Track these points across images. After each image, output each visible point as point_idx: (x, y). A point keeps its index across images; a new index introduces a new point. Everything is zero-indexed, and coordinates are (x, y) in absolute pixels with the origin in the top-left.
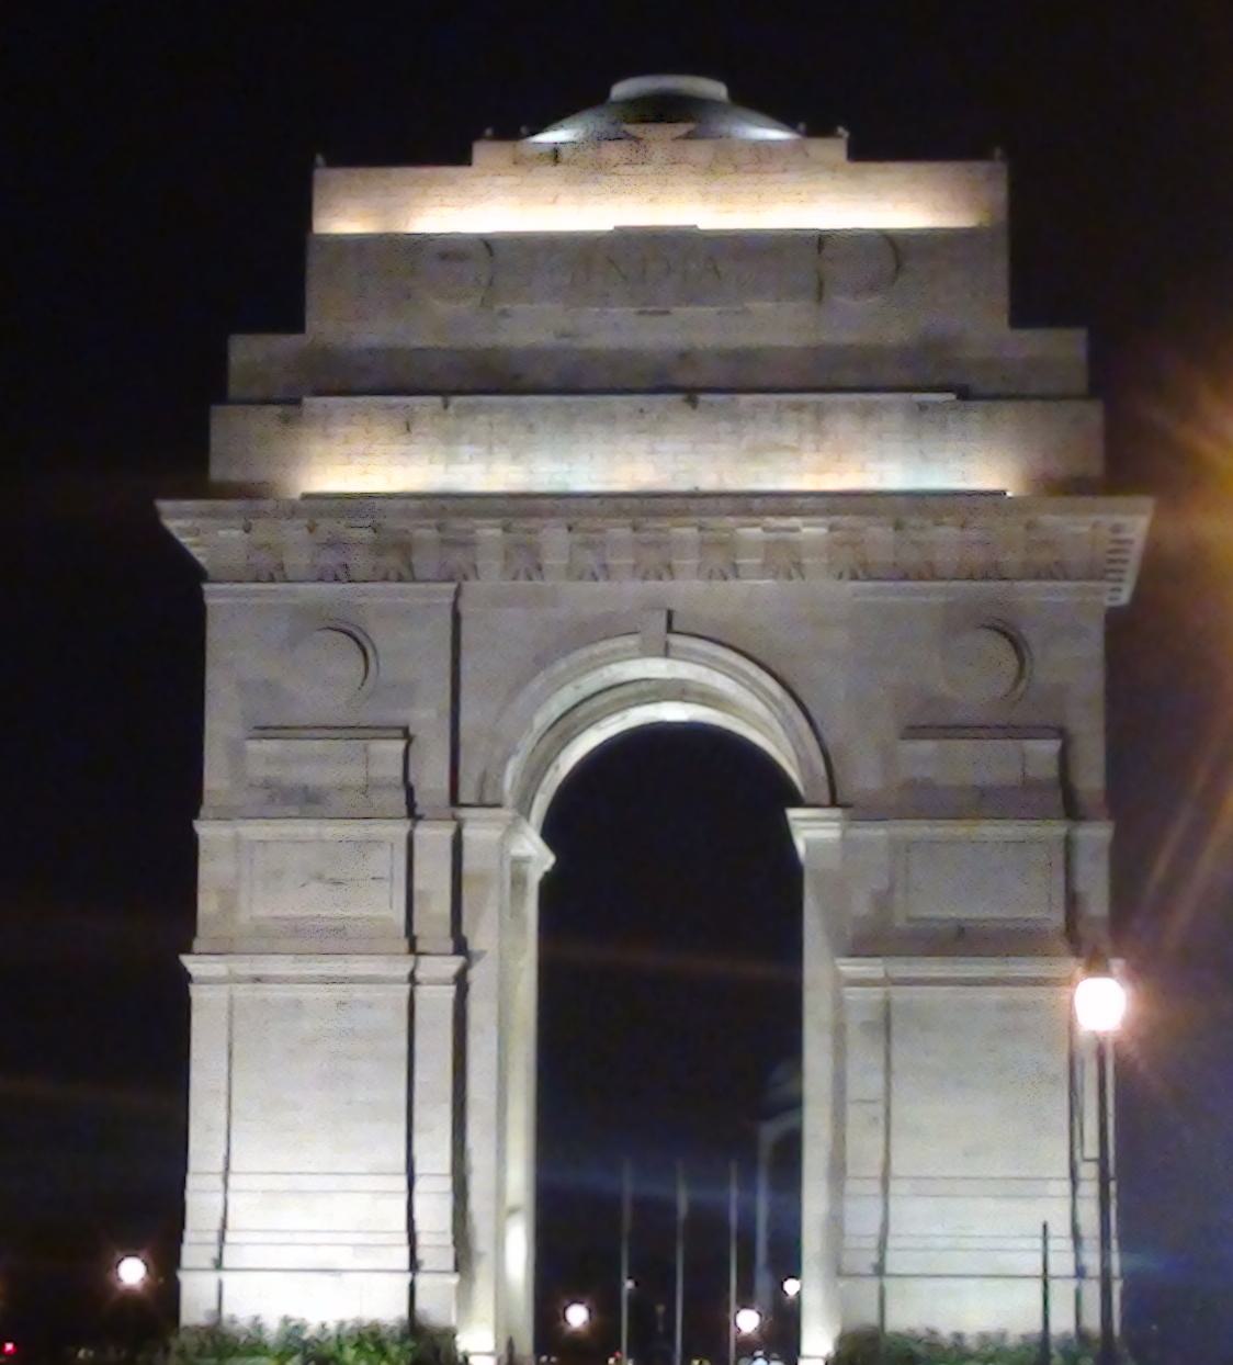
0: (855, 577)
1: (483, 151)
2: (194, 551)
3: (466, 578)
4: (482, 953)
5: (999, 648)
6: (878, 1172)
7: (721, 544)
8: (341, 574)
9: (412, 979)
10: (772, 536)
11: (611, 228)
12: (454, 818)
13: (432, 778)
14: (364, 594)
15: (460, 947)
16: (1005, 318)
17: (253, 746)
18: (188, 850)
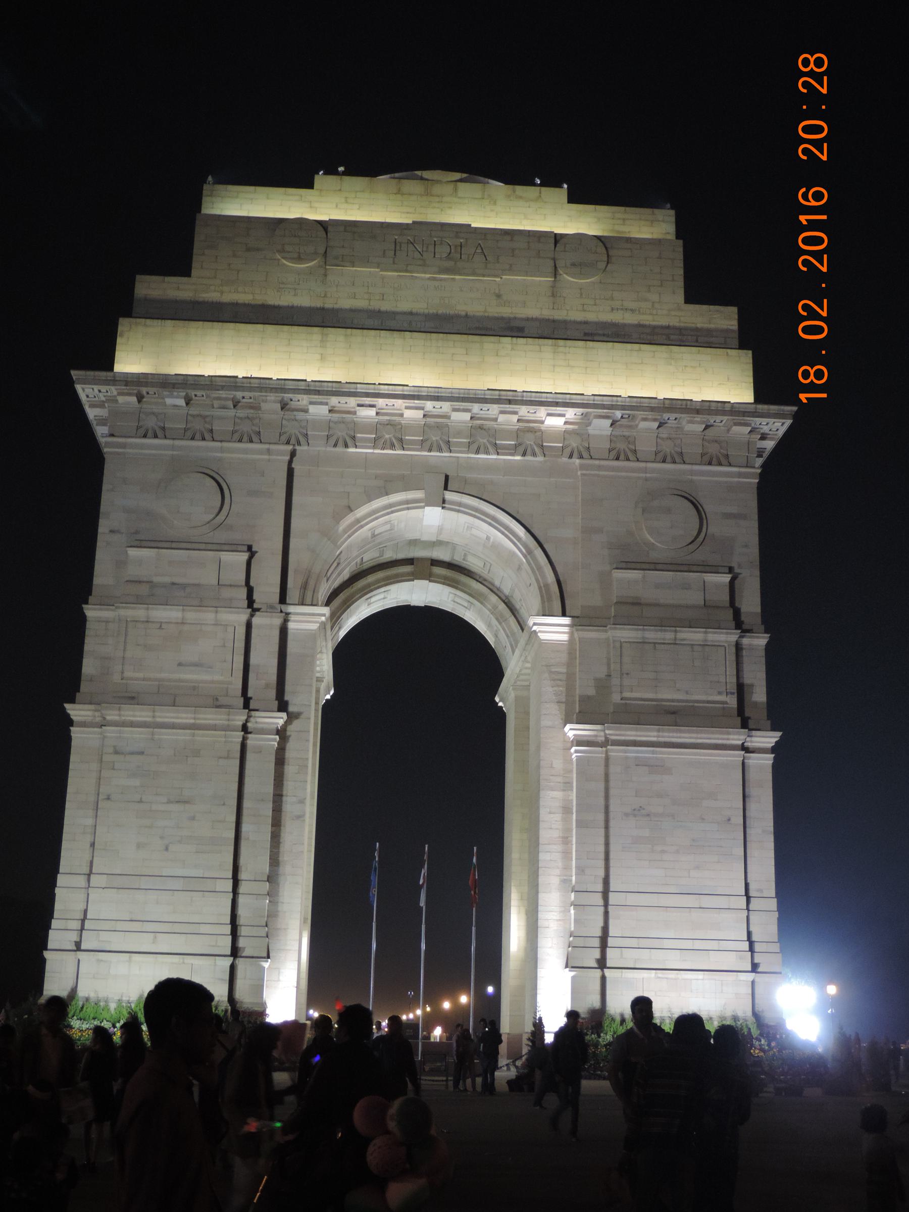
0: (581, 457)
1: (320, 179)
2: (100, 431)
3: (299, 444)
6: (600, 887)
8: (207, 436)
11: (408, 221)
12: (281, 612)
14: (222, 450)
15: (283, 706)
16: (680, 297)
17: (132, 552)
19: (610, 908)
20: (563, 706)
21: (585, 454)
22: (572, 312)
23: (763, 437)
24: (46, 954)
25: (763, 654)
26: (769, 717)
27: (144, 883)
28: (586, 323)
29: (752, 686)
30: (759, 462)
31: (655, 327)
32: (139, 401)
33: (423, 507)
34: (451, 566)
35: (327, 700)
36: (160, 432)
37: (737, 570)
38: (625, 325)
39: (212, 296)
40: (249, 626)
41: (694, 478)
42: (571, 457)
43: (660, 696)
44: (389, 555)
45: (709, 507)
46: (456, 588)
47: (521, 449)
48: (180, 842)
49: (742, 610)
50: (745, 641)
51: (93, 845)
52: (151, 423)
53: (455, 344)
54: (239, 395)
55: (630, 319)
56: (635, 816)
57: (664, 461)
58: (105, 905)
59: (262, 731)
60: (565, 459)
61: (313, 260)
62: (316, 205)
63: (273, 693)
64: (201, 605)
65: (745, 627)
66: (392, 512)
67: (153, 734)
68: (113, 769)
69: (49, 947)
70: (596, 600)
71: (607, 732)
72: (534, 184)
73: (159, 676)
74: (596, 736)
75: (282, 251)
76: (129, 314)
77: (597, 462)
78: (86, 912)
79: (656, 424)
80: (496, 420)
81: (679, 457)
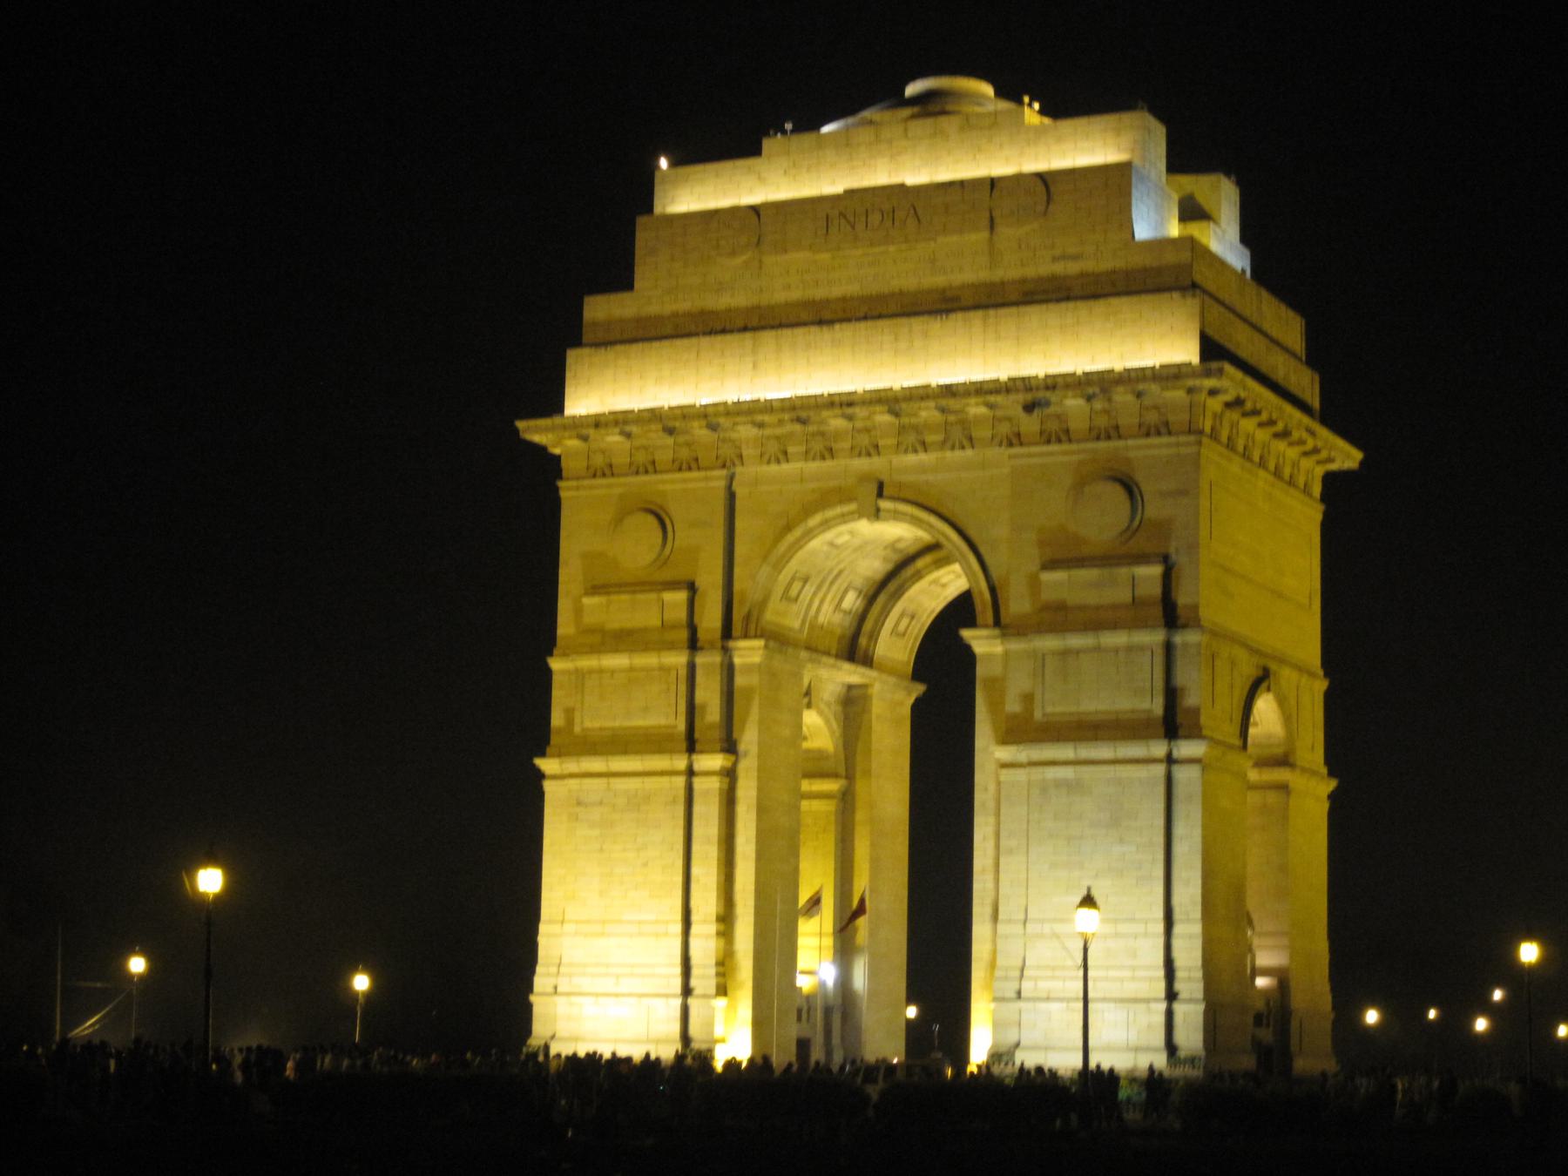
0: (1011, 444)
5: (1117, 493)
6: (1022, 917)
9: (690, 773)
13: (710, 619)
14: (664, 482)
17: (586, 601)
18: (544, 678)
22: (1011, 270)
24: (533, 998)
28: (1024, 281)
36: (609, 471)
37: (1174, 557)
38: (1065, 278)
39: (654, 309)
40: (692, 668)
45: (1148, 488)
52: (599, 461)
55: (1073, 268)
81: (1113, 432)
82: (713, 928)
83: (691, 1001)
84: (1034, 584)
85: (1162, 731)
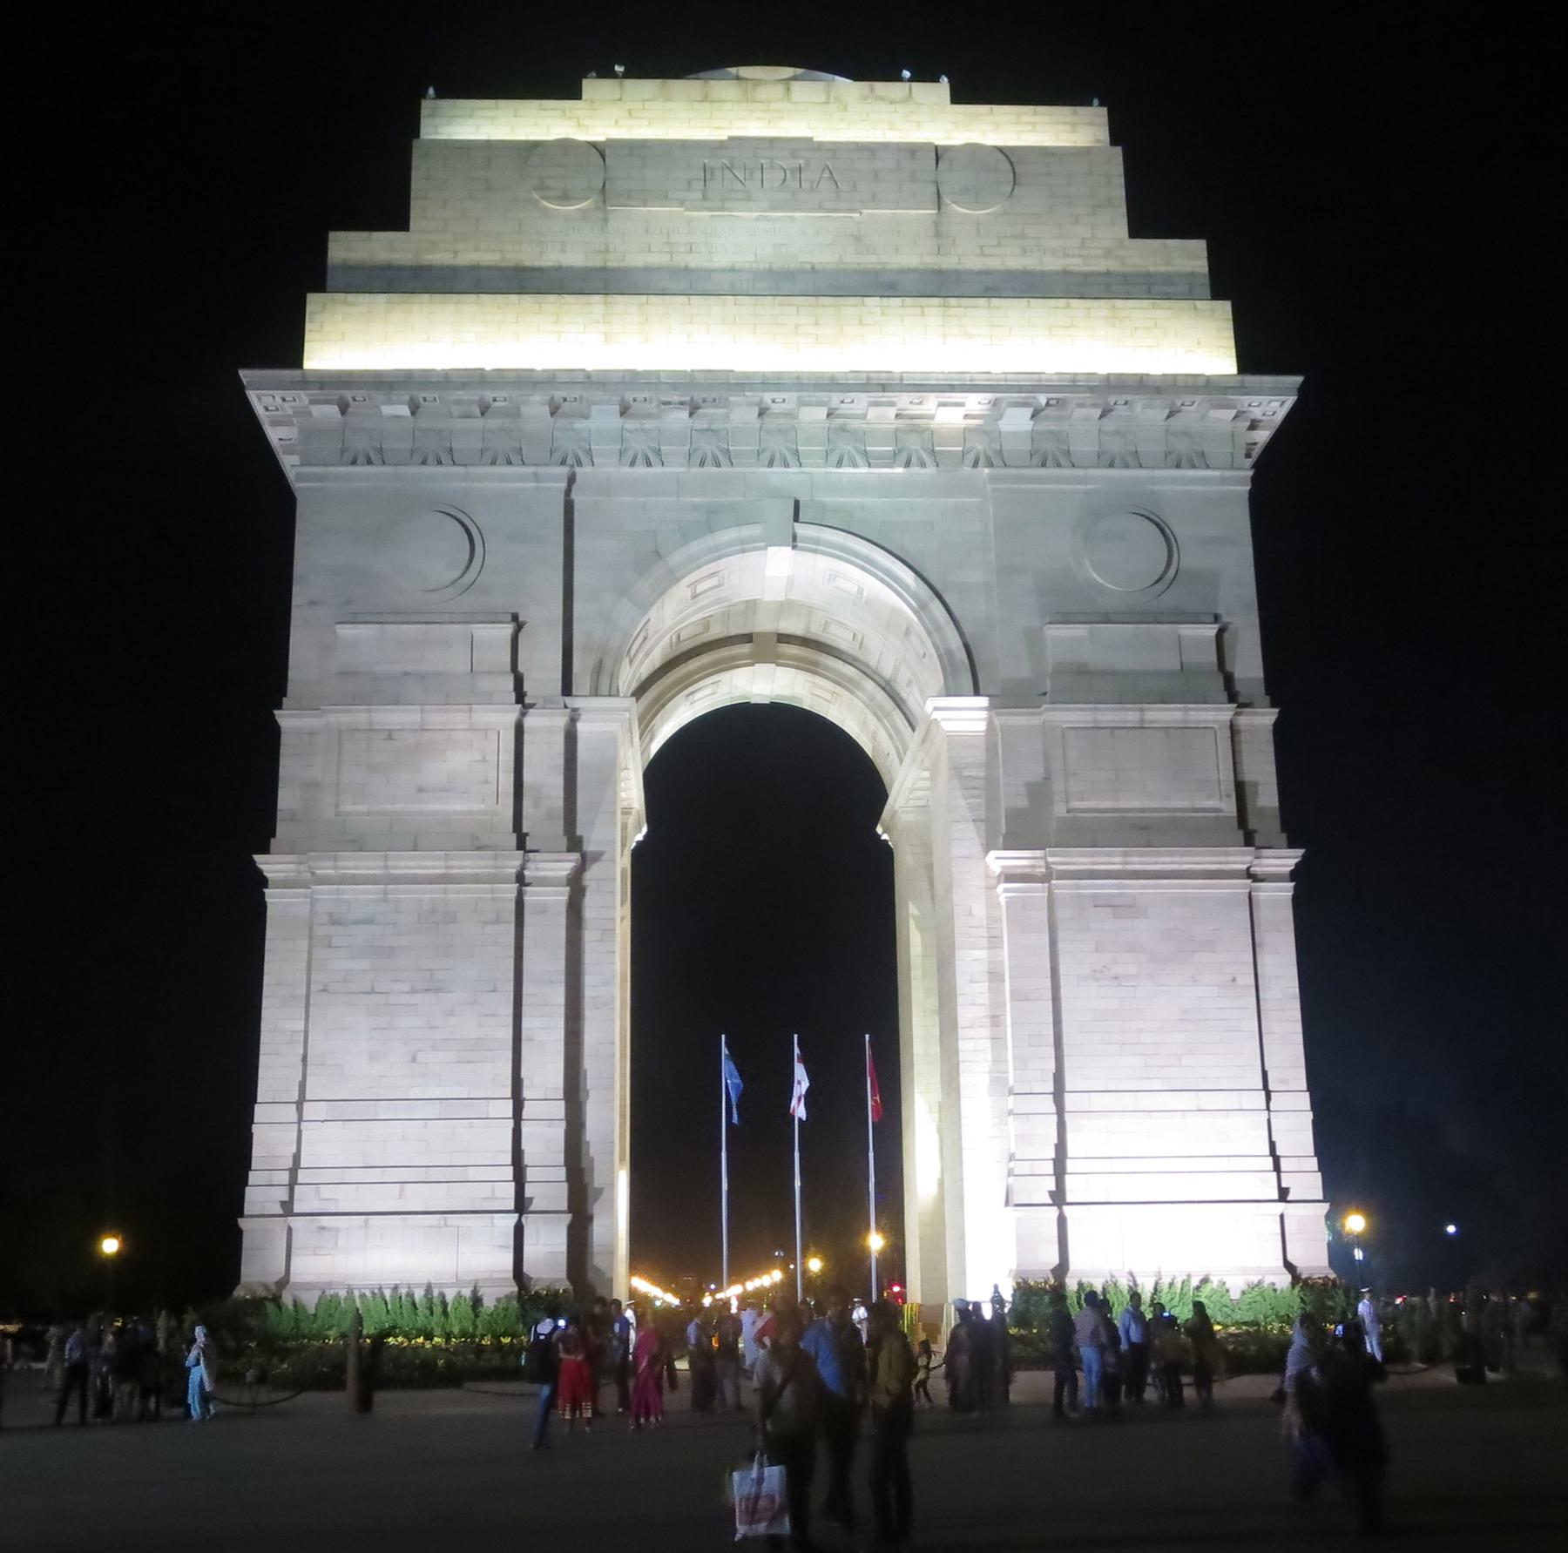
0: (990, 465)
1: (590, 86)
2: (290, 464)
3: (580, 464)
4: (597, 857)
7: (853, 432)
9: (520, 879)
10: (902, 423)
11: (722, 135)
15: (575, 844)
16: (1122, 229)
17: (345, 631)
18: (269, 741)
19: (1067, 1117)
20: (983, 826)
21: (996, 461)
23: (1254, 425)
24: (243, 1223)
25: (1269, 737)
26: (1283, 830)
27: (384, 1110)
29: (1255, 785)
30: (1250, 462)
31: (1087, 275)
32: (343, 412)
33: (765, 548)
34: (804, 642)
35: (639, 843)
37: (1225, 619)
38: (1043, 274)
40: (519, 730)
41: (1156, 488)
42: (975, 464)
43: (1123, 805)
44: (716, 632)
46: (816, 673)
47: (903, 458)
48: (434, 1049)
49: (1237, 675)
50: (1243, 721)
51: (305, 1058)
52: (361, 444)
53: (800, 312)
54: (489, 395)
55: (1053, 264)
56: (1096, 979)
57: (1111, 465)
58: (325, 1145)
59: (545, 882)
60: (968, 469)
61: (586, 199)
62: (587, 122)
63: (559, 826)
64: (447, 701)
65: (1241, 700)
66: (720, 558)
67: (385, 893)
68: (330, 947)
69: (246, 1212)
70: (1025, 672)
71: (1050, 859)
72: (899, 79)
73: (389, 807)
74: (1032, 867)
75: (541, 187)
76: (321, 288)
77: (1014, 471)
78: (297, 1158)
79: (1098, 412)
80: (864, 416)
81: (1135, 460)
82: (559, 1109)
83: (528, 1220)
84: (1034, 640)
85: (1240, 835)
